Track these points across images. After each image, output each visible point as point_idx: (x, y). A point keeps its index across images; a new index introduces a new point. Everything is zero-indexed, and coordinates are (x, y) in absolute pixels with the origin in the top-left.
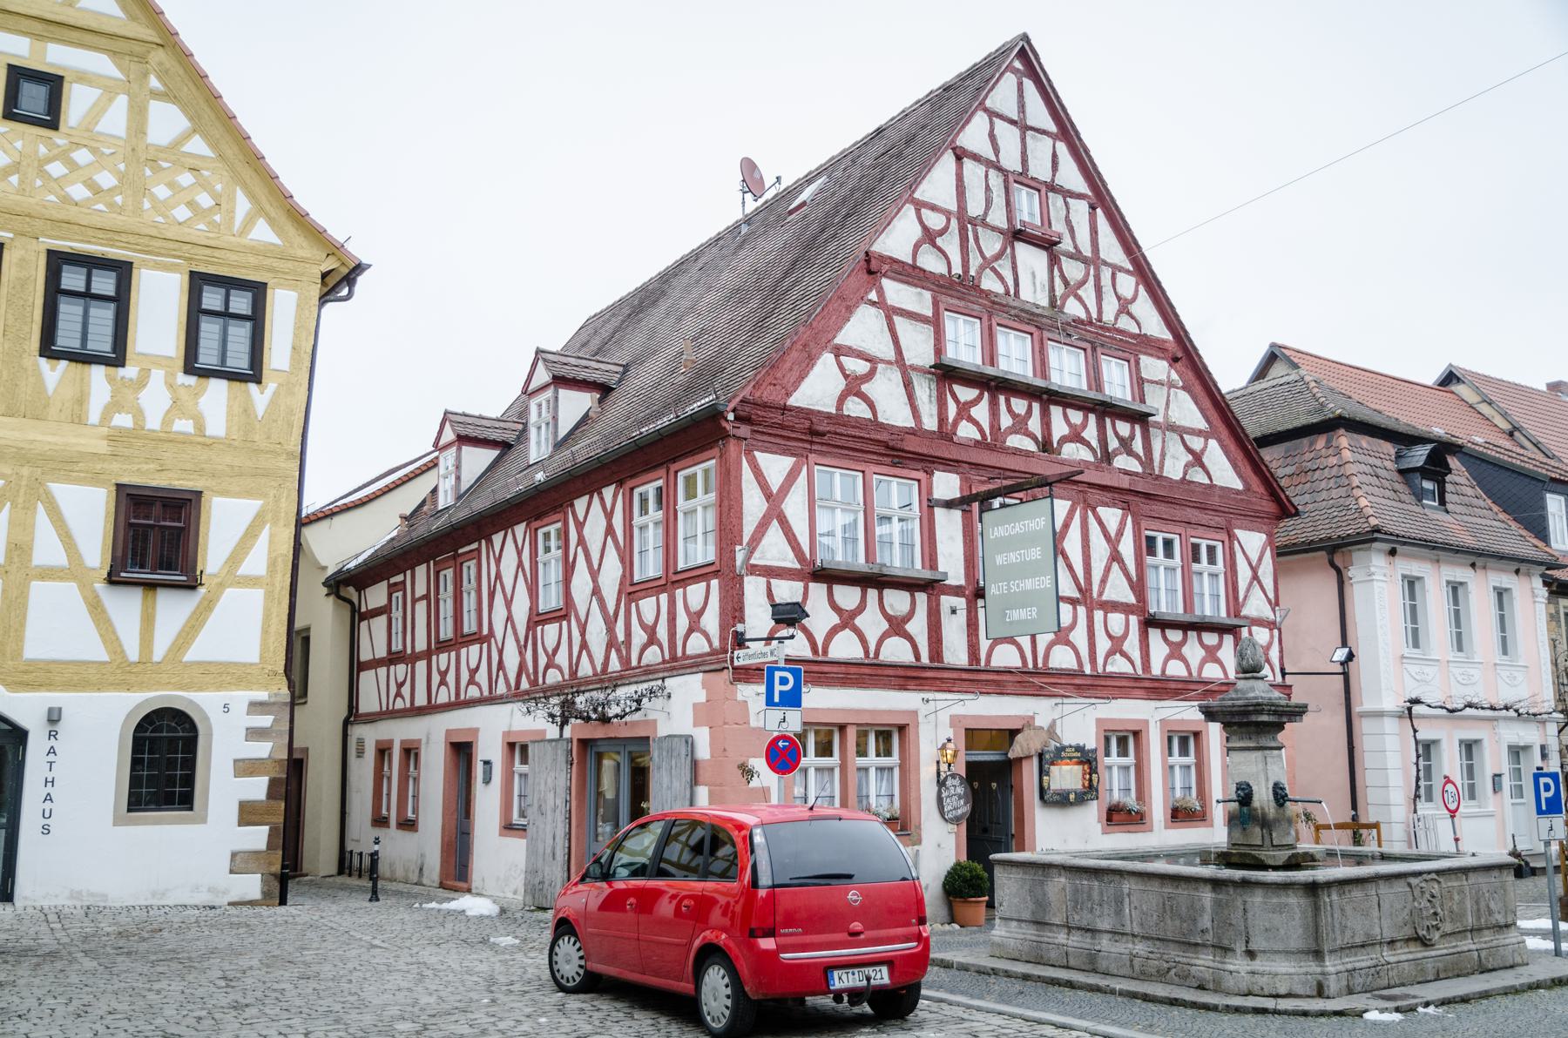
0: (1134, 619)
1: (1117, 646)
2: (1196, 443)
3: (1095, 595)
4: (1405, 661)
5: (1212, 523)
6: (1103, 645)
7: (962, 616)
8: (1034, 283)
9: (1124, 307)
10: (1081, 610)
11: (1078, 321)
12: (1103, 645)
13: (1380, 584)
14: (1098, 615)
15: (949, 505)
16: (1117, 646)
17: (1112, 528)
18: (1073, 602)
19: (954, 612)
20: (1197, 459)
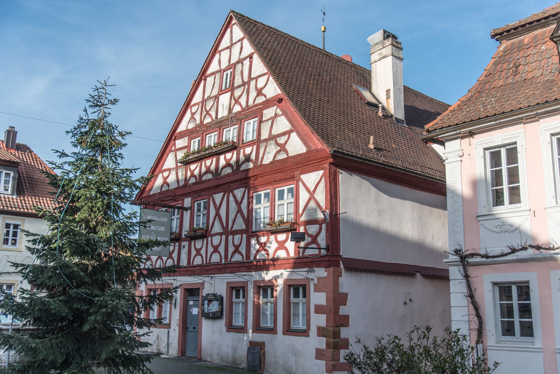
0: (244, 236)
1: (237, 250)
2: (282, 140)
3: (229, 229)
4: (480, 219)
5: (287, 177)
6: (231, 249)
7: (187, 247)
8: (223, 109)
9: (260, 92)
10: (224, 237)
11: (239, 112)
12: (231, 249)
13: (451, 165)
14: (230, 237)
15: (186, 209)
16: (237, 250)
17: (239, 197)
18: (220, 234)
19: (184, 247)
20: (283, 148)
